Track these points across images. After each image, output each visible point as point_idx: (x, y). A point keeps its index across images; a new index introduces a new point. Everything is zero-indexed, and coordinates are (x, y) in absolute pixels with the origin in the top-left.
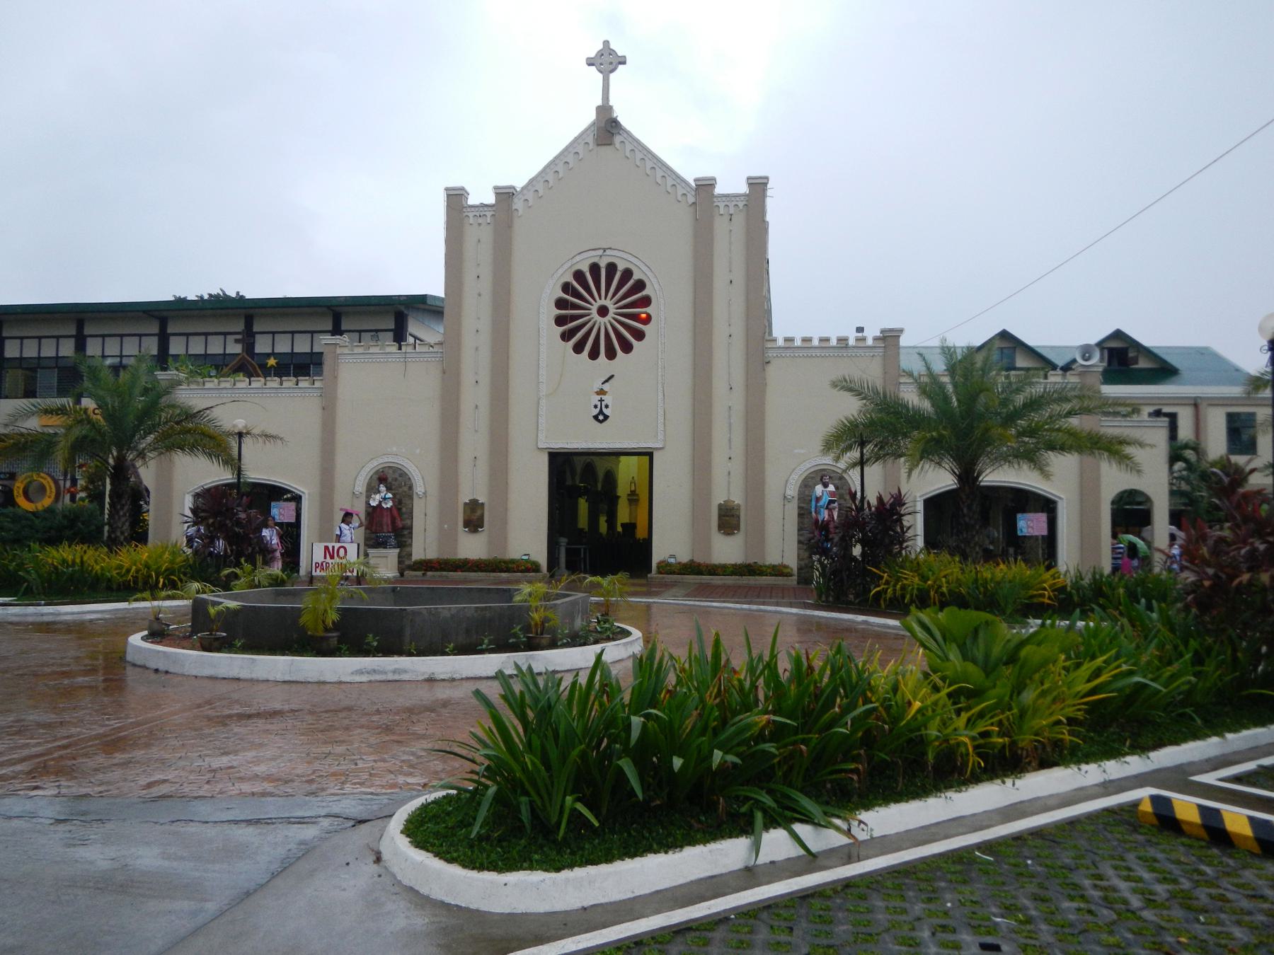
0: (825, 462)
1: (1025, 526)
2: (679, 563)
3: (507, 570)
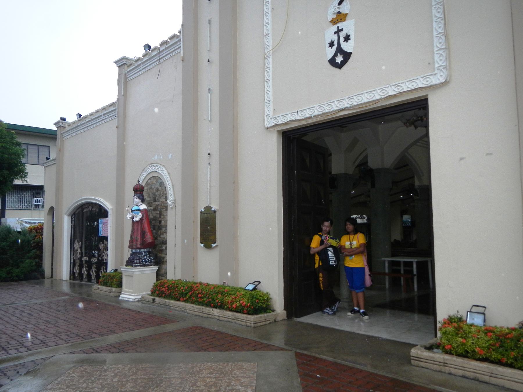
2: (488, 331)
3: (221, 306)
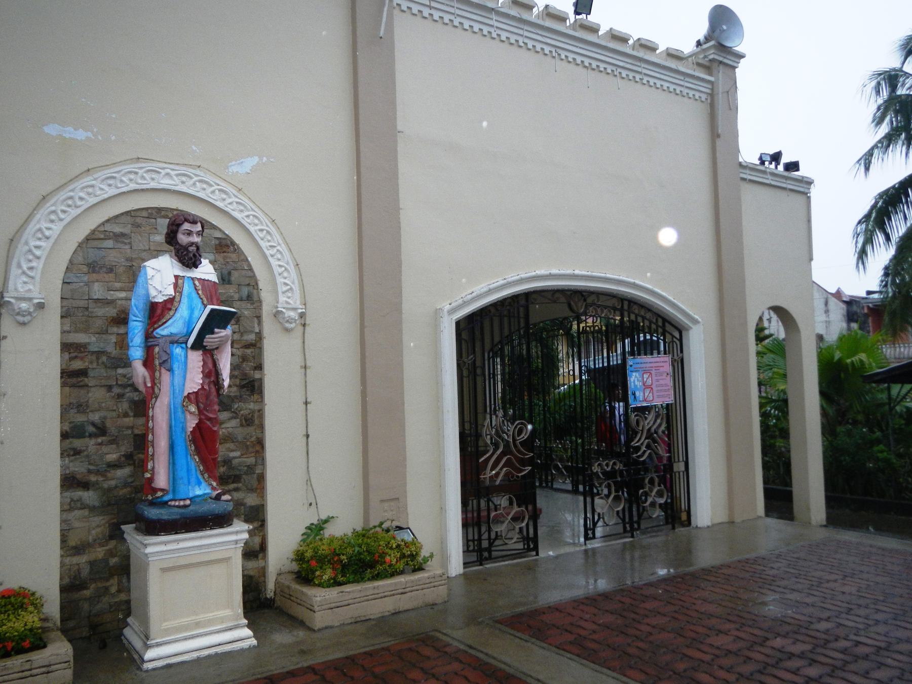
0: (165, 183)
1: (639, 384)
